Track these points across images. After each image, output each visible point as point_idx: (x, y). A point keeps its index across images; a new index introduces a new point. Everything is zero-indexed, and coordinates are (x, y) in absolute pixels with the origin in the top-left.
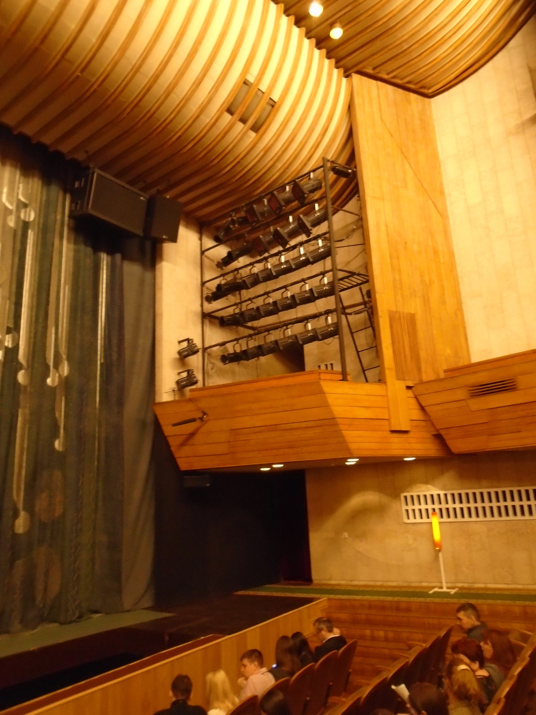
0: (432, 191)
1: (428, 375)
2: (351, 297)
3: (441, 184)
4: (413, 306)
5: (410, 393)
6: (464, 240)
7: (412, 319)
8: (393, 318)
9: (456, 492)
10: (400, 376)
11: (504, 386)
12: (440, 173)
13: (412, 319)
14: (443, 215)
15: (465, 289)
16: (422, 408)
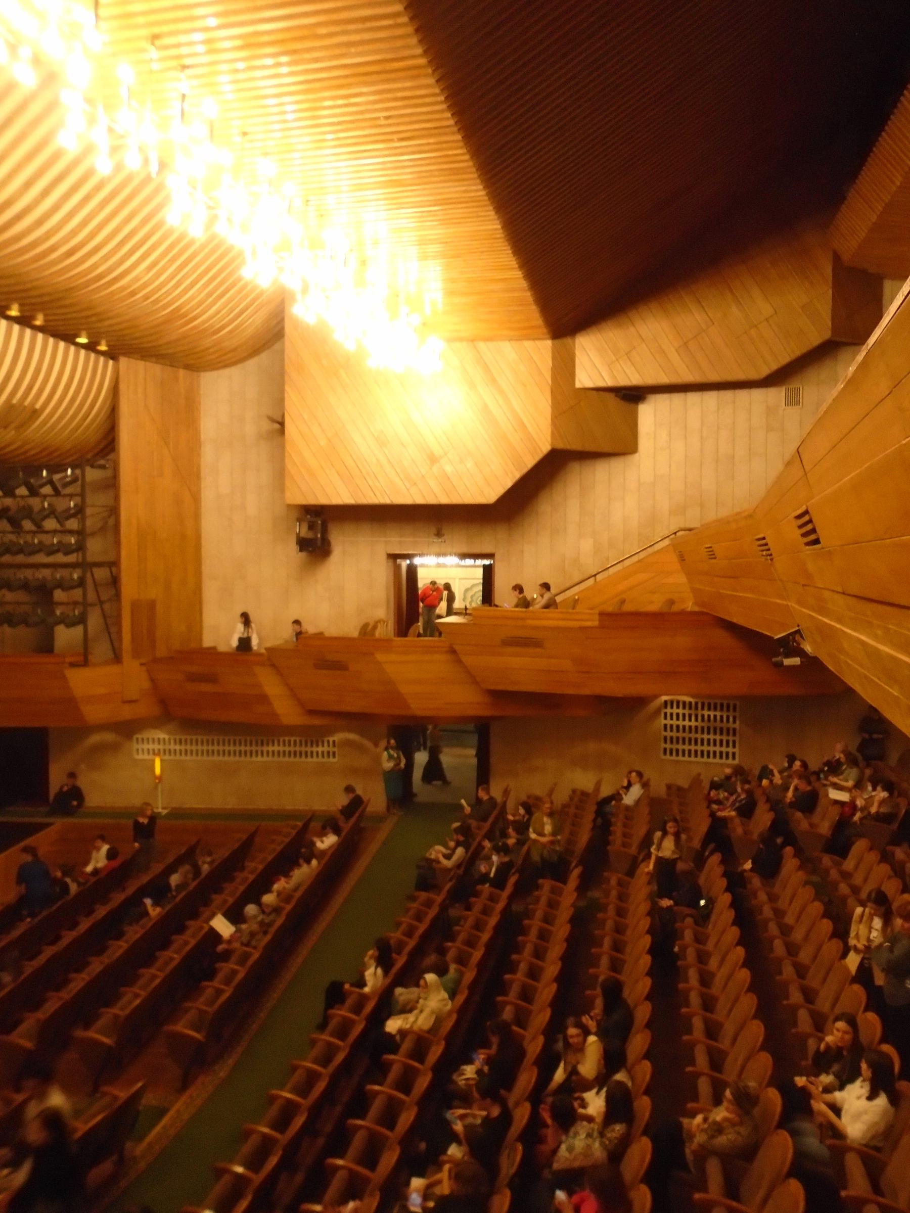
0: (189, 475)
1: (161, 651)
2: (101, 574)
3: (199, 467)
4: (154, 592)
5: (144, 668)
6: (211, 525)
7: (152, 605)
8: (135, 605)
9: (178, 737)
10: (136, 654)
11: (212, 679)
12: (199, 455)
13: (152, 605)
14: (196, 499)
15: (206, 570)
16: (152, 680)
